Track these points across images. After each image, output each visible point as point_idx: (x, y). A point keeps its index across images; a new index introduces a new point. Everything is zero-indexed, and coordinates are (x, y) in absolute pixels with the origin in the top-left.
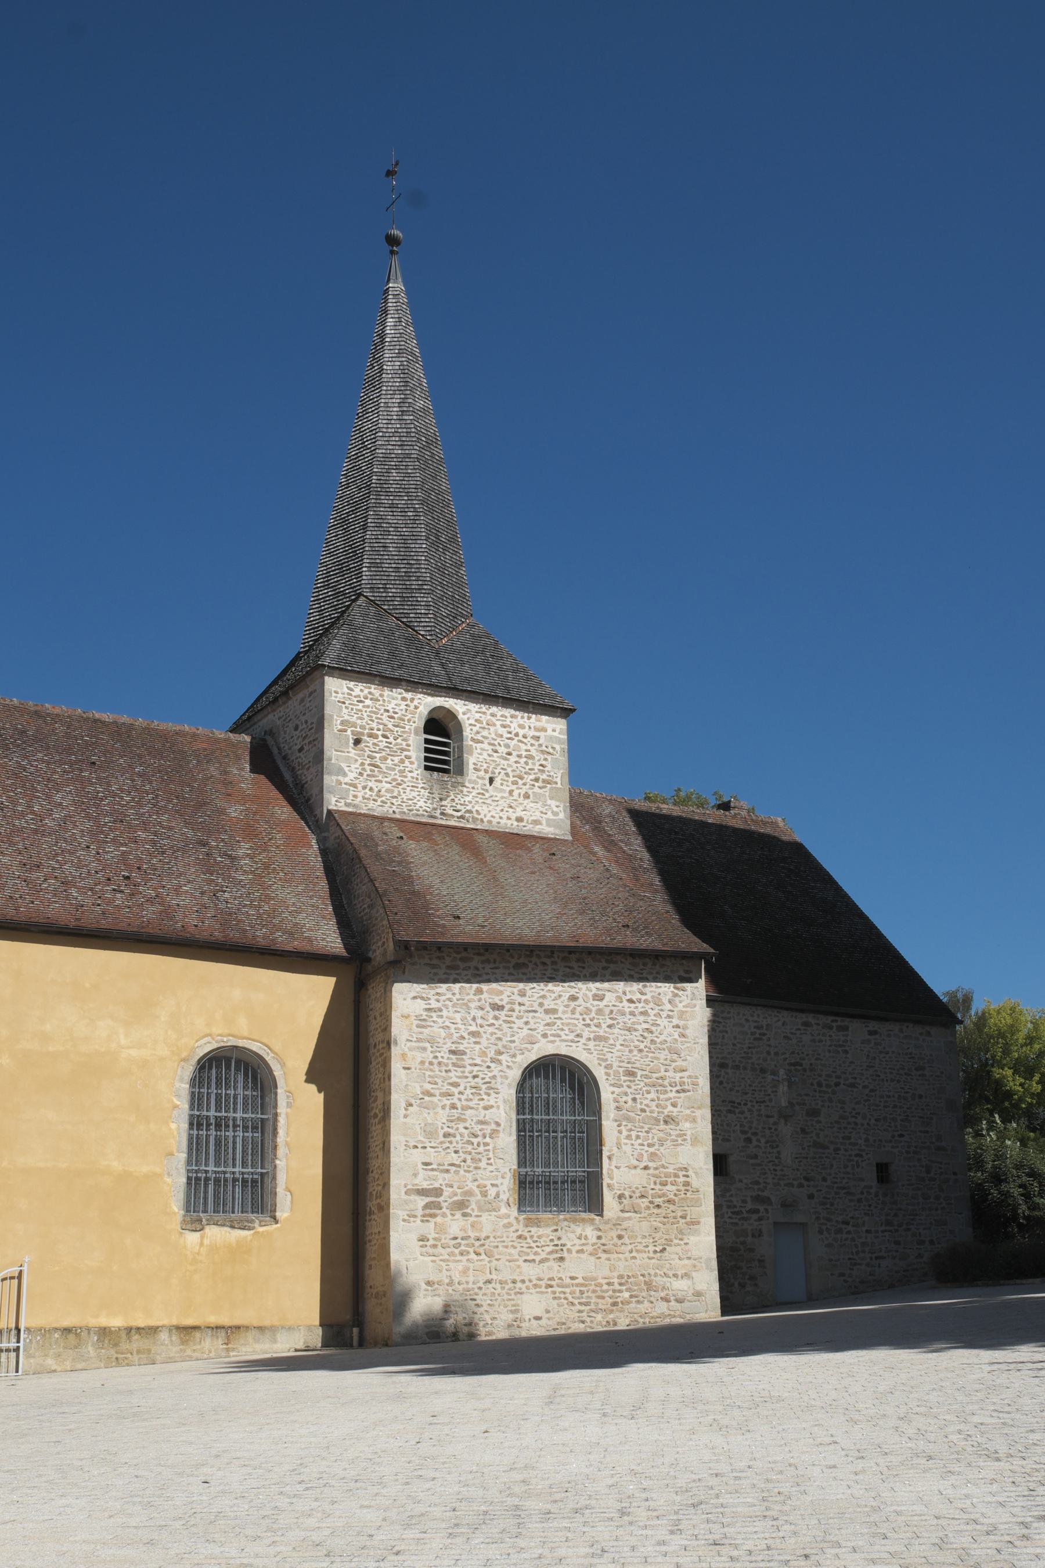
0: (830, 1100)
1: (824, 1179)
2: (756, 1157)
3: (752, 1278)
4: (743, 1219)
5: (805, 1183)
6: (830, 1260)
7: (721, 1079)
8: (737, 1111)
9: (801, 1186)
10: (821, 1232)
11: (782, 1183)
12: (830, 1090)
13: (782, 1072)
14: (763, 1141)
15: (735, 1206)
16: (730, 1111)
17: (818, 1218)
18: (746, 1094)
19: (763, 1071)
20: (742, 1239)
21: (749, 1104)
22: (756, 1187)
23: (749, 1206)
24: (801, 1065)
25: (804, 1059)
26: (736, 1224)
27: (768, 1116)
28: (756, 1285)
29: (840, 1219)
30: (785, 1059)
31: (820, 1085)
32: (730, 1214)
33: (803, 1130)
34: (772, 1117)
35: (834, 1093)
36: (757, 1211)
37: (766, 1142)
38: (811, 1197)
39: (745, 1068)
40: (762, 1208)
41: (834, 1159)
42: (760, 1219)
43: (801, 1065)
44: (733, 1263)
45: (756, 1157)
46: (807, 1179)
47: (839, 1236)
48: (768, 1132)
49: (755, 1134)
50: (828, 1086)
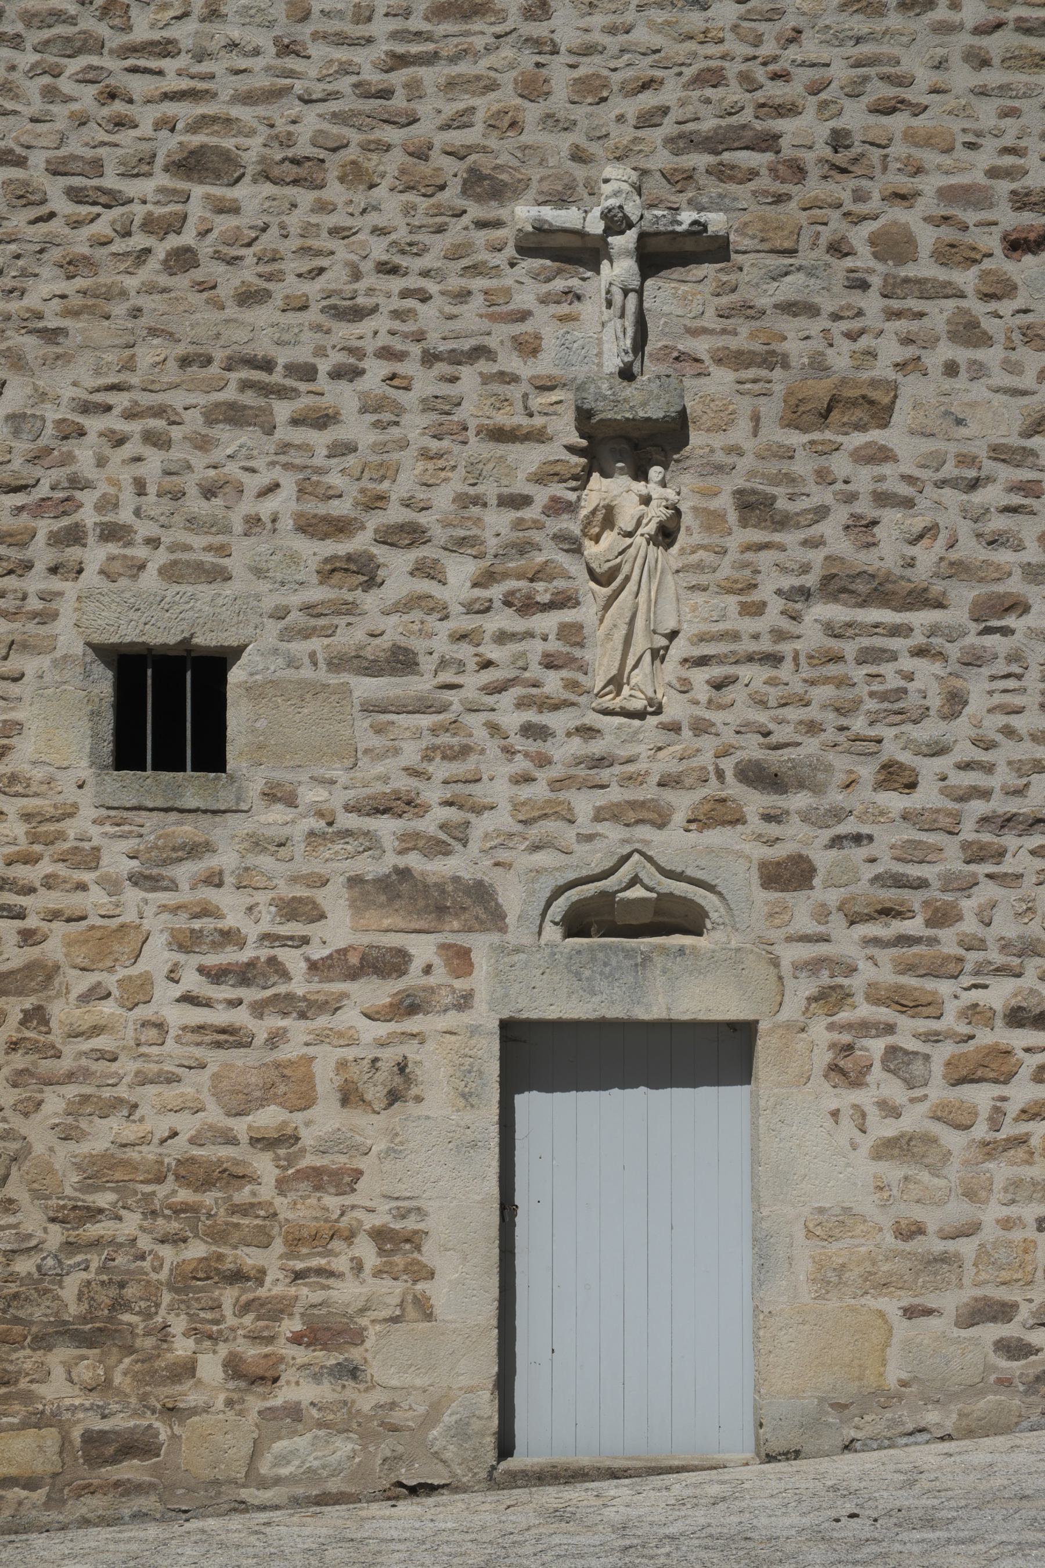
0: (967, 331)
1: (897, 777)
2: (402, 661)
3: (325, 1332)
4: (285, 1004)
5: (755, 802)
6: (913, 1231)
7: (188, 238)
8: (282, 410)
9: (719, 815)
10: (844, 1071)
11: (584, 804)
12: (967, 279)
13: (616, 179)
14: (460, 571)
15: (229, 937)
16: (234, 415)
17: (830, 998)
18: (357, 314)
19: (487, 186)
20: (269, 1118)
21: (376, 370)
22: (386, 827)
23: (339, 930)
24: (769, 142)
25: (787, 110)
26: (230, 1037)
27: (500, 435)
28: (353, 1372)
29: (999, 995)
30: (649, 120)
31: (894, 246)
32: (191, 981)
33: (753, 506)
34: (538, 436)
35: (997, 291)
36: (389, 964)
38: (789, 875)
39: (357, 176)
40: (423, 949)
41: (974, 660)
42: (409, 1006)
43: (769, 142)
44: (196, 1250)
45: (402, 661)
46: (756, 776)
47: (981, 1096)
48: (497, 523)
49: (411, 535)
50: (949, 254)
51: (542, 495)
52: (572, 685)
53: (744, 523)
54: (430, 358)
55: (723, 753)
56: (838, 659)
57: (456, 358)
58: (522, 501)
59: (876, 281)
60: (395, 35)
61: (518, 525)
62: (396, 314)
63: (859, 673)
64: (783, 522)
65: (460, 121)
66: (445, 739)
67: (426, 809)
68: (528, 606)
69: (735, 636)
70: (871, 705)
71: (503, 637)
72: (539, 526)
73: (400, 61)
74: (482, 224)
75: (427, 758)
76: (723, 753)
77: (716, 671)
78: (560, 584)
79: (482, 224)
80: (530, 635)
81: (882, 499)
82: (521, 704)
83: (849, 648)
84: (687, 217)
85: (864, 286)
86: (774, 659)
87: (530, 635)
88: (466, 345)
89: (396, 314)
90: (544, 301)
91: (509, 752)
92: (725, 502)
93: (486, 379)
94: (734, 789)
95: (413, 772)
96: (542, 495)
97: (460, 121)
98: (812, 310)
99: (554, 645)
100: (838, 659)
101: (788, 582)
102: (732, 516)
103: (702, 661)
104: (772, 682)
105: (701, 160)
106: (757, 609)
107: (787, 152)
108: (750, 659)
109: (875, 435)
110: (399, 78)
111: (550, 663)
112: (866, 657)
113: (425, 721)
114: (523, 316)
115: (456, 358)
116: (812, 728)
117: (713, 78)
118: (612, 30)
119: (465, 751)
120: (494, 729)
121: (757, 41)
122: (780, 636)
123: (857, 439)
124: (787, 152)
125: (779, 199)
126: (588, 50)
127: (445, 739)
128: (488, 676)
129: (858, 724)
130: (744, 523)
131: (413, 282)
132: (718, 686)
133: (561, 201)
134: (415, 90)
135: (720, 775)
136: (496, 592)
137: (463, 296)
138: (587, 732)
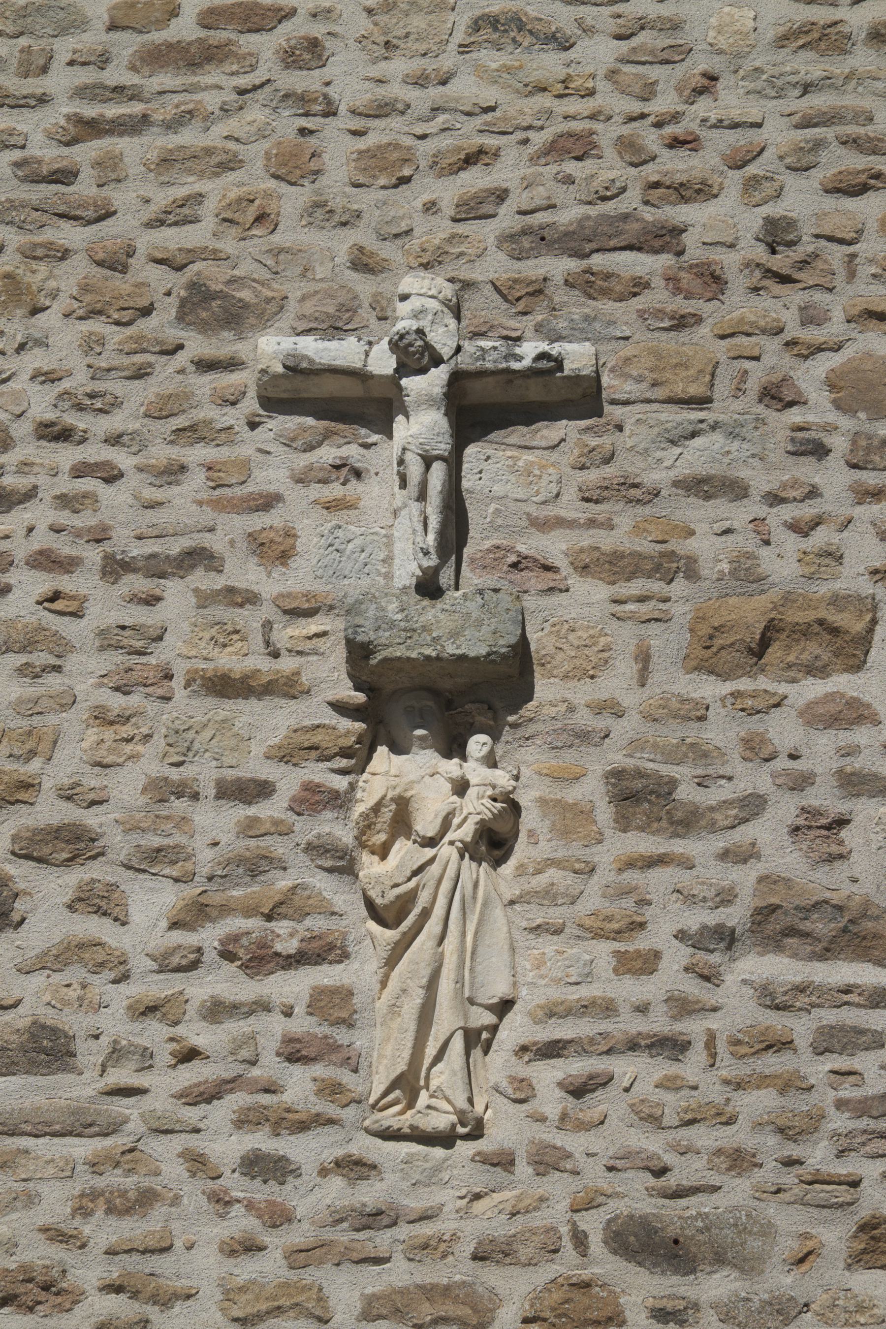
14: (151, 903)
19: (215, 308)
24: (666, 239)
27: (223, 686)
30: (472, 209)
33: (638, 797)
34: (287, 688)
37: (193, 915)
48: (215, 826)
49: (71, 844)
51: (289, 781)
52: (331, 1090)
53: (624, 824)
54: (115, 568)
55: (584, 1205)
56: (782, 1045)
57: (158, 568)
58: (258, 790)
59: (839, 443)
60: (81, 92)
61: (249, 829)
62: (64, 501)
63: (816, 1070)
64: (687, 822)
65: (180, 214)
66: (114, 1179)
67: (76, 1297)
68: (260, 960)
69: (607, 1008)
70: (840, 1122)
71: (217, 1011)
72: (283, 831)
73: (90, 128)
74: (206, 366)
75: (82, 1211)
76: (584, 1205)
77: (576, 1067)
78: (317, 923)
79: (206, 366)
80: (262, 1006)
81: (854, 783)
82: (244, 1121)
83: (801, 1028)
84: (529, 349)
85: (820, 451)
86: (673, 1046)
87: (262, 1006)
88: (175, 547)
89: (64, 501)
90: (301, 479)
91: (221, 1201)
92: (592, 790)
93: (205, 599)
94: (604, 1265)
95: (57, 1235)
96: (289, 781)
97: (180, 214)
98: (736, 490)
99: (303, 1024)
100: (782, 1045)
101: (697, 919)
102: (605, 813)
103: (552, 1050)
104: (669, 1084)
105: (558, 267)
106: (646, 964)
107: (694, 252)
108: (633, 1046)
109: (842, 683)
110: (85, 154)
111: (295, 1053)
112: (829, 1042)
113: (81, 1149)
114: (268, 502)
115: (158, 568)
116: (739, 1161)
117: (578, 146)
118: (420, 81)
119: (146, 1199)
120: (197, 1162)
121: (648, 92)
122: (683, 1007)
123: (812, 689)
124: (694, 252)
125: (682, 323)
126: (382, 110)
127: (114, 1179)
128: (190, 1075)
129: (819, 1155)
130: (624, 824)
131: (95, 452)
132: (578, 1090)
133: (334, 330)
134: (110, 170)
135: (580, 1240)
136: (209, 936)
137: (174, 472)
138: (355, 1168)
